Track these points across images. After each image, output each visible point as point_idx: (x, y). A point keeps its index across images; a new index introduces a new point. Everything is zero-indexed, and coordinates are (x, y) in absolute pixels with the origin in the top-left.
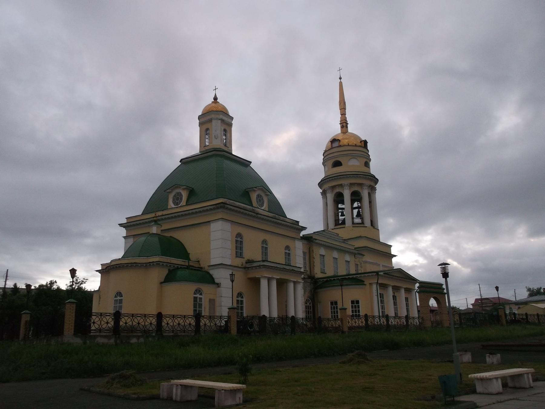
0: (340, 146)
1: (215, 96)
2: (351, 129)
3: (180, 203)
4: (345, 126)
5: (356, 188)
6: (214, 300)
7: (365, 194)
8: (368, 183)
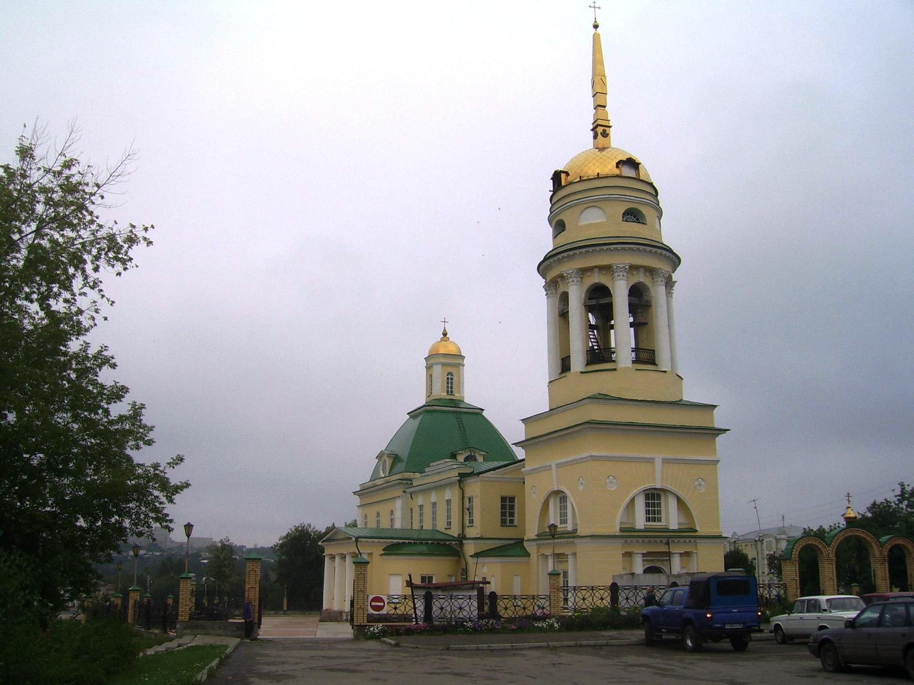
4: (599, 134)
5: (641, 278)
7: (658, 291)
8: (664, 267)
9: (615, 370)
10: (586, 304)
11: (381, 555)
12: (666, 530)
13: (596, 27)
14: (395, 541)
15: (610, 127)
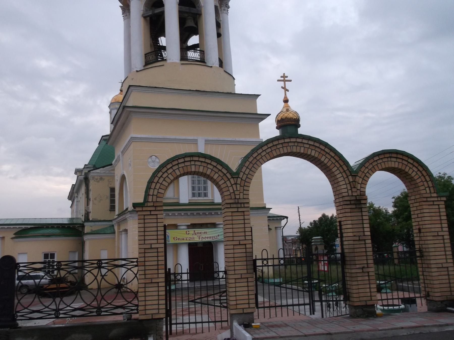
10: (144, 16)
11: (12, 238)
12: (213, 204)
14: (23, 226)
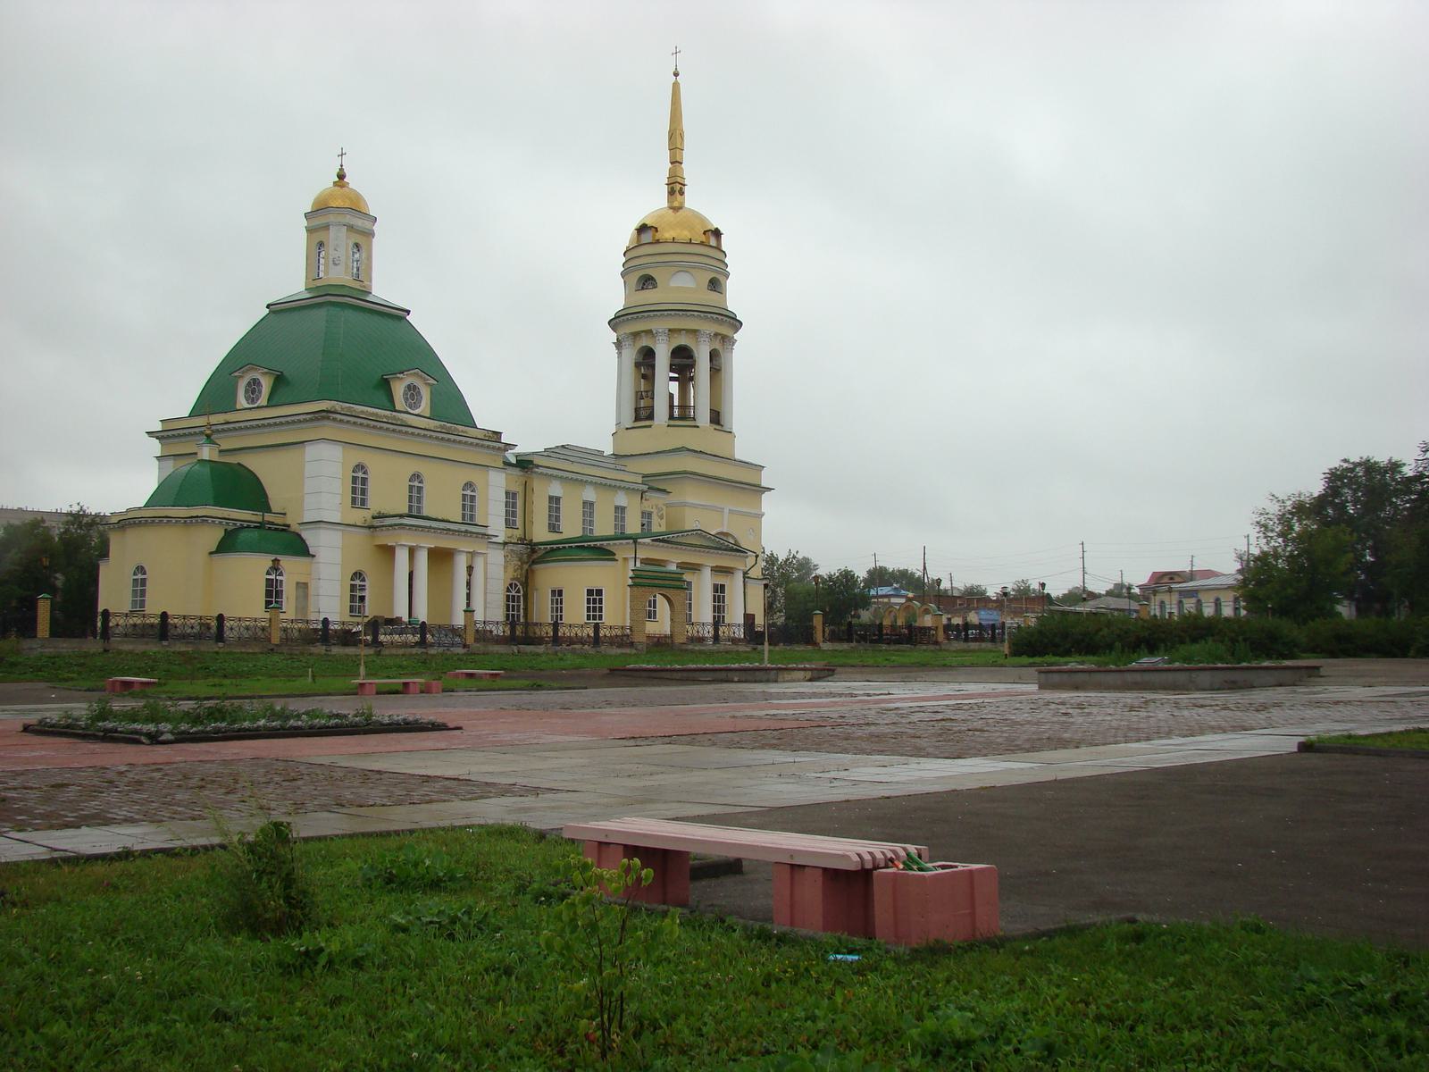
0: (658, 242)
1: (341, 169)
2: (691, 200)
3: (257, 400)
5: (683, 340)
6: (306, 585)
8: (708, 328)
9: (650, 426)
13: (676, 74)
15: (684, 185)
